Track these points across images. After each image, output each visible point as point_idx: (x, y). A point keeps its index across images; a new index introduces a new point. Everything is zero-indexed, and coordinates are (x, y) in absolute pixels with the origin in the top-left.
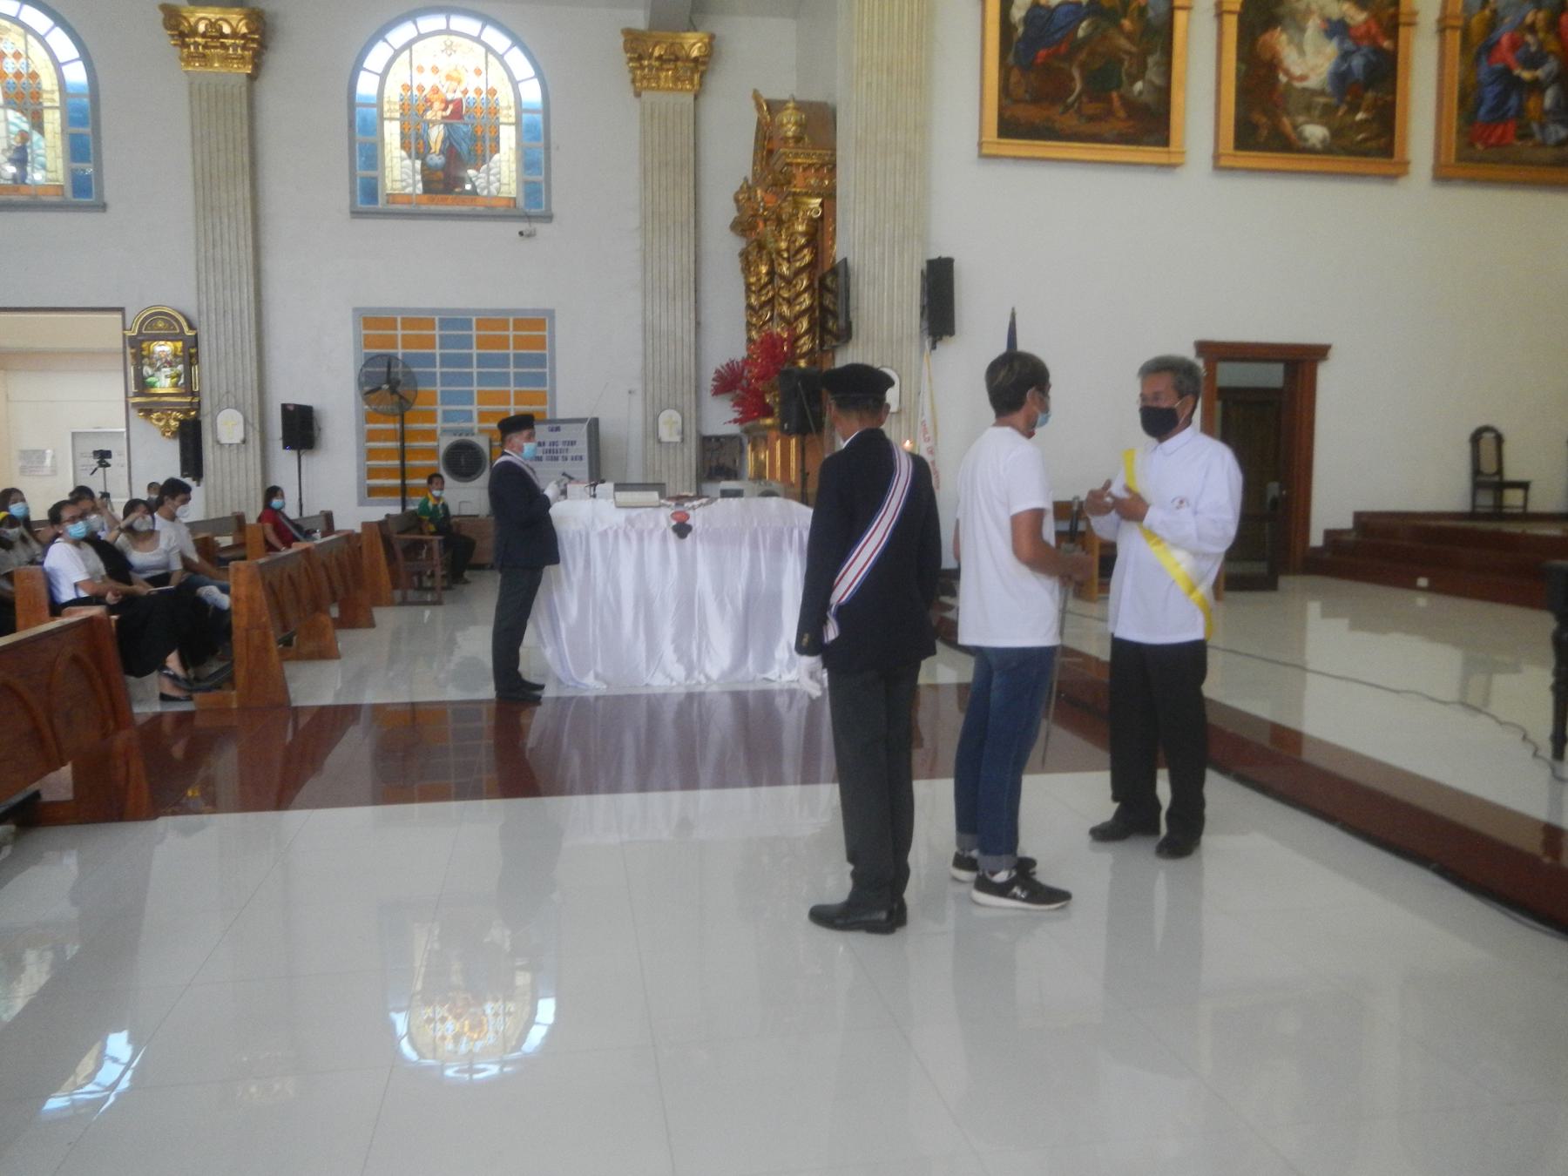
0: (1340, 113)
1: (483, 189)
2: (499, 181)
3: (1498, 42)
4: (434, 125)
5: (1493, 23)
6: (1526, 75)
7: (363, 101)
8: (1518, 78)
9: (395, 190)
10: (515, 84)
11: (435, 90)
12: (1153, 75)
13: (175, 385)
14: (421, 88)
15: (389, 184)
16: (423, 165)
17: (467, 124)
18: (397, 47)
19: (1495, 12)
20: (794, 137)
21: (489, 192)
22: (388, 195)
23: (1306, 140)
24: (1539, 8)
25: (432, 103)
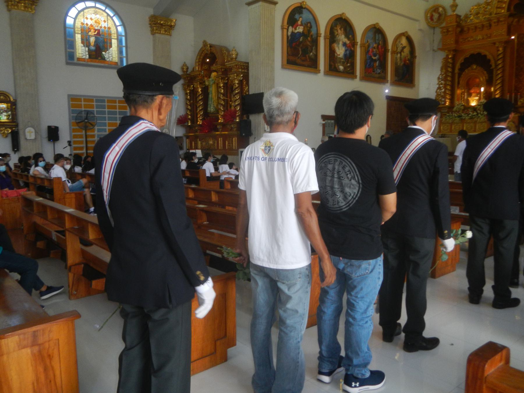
0: (345, 64)
1: (108, 58)
2: (112, 56)
3: (370, 50)
4: (92, 37)
5: (369, 46)
6: (374, 58)
7: (69, 27)
8: (372, 58)
9: (79, 57)
10: (116, 27)
11: (92, 25)
12: (314, 51)
13: (8, 119)
14: (87, 24)
15: (78, 55)
16: (89, 49)
17: (102, 38)
18: (79, 10)
19: (369, 44)
20: (235, 58)
21: (109, 60)
22: (78, 58)
23: (340, 69)
24: (376, 43)
25: (91, 30)
